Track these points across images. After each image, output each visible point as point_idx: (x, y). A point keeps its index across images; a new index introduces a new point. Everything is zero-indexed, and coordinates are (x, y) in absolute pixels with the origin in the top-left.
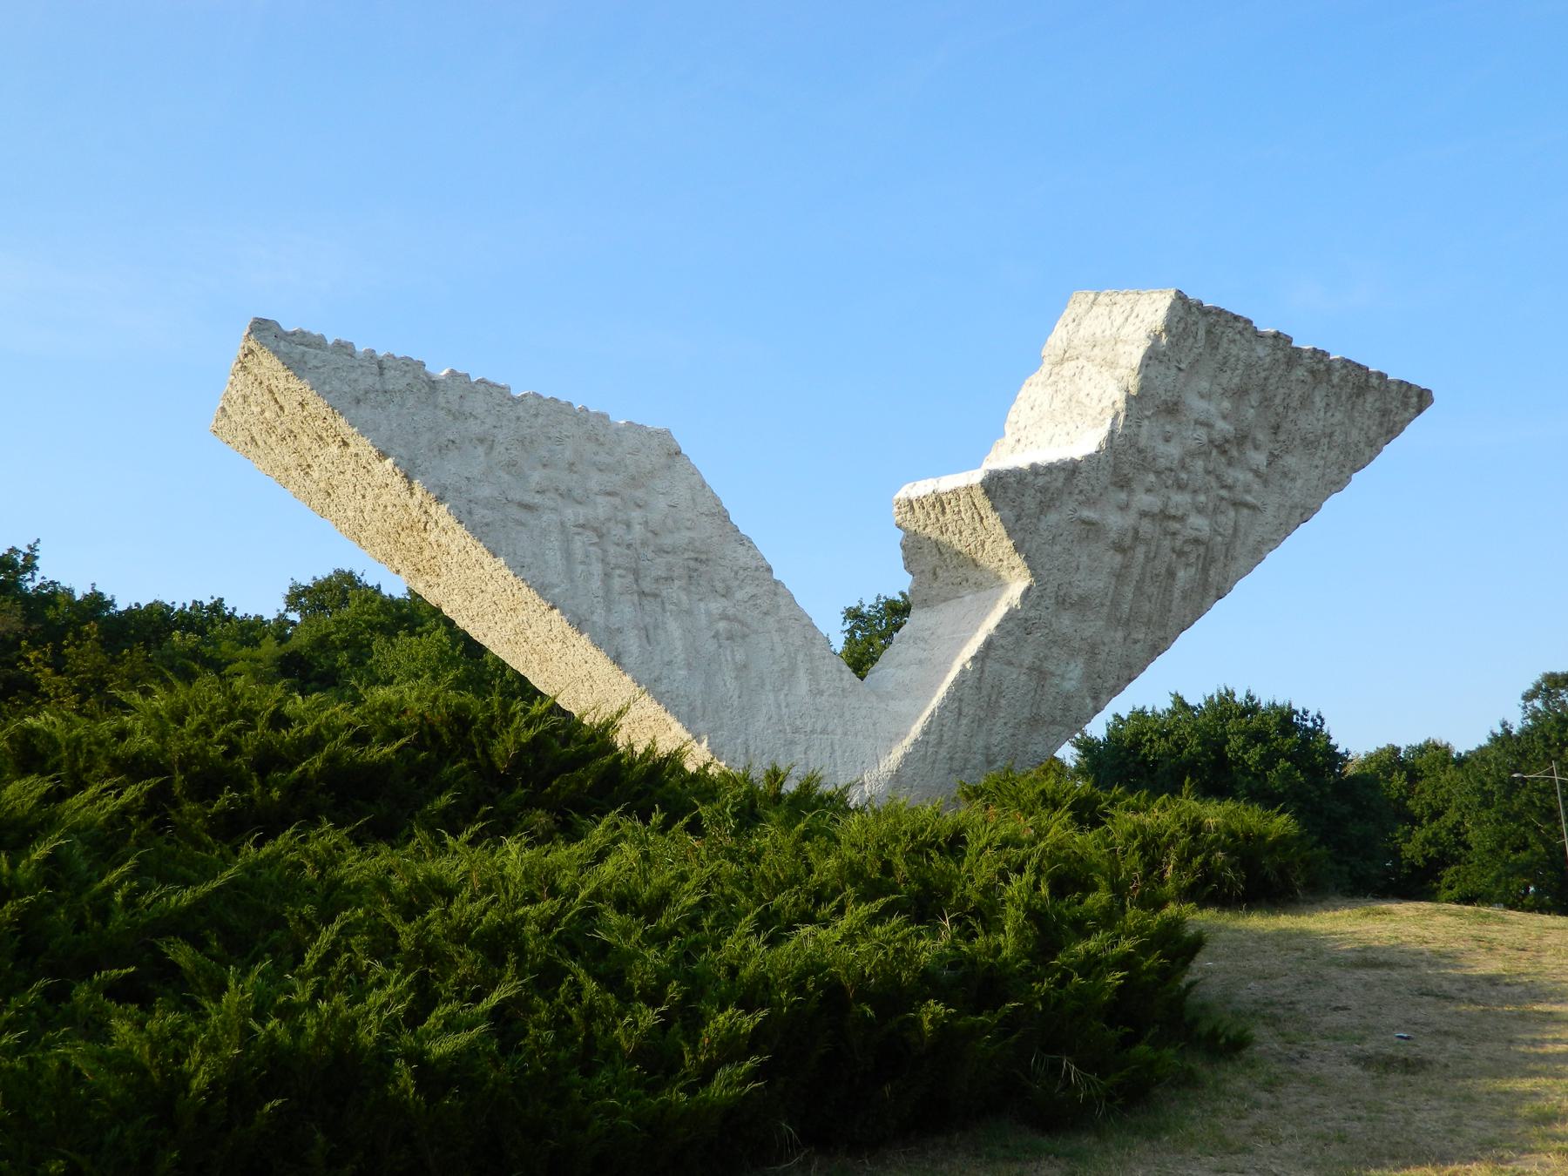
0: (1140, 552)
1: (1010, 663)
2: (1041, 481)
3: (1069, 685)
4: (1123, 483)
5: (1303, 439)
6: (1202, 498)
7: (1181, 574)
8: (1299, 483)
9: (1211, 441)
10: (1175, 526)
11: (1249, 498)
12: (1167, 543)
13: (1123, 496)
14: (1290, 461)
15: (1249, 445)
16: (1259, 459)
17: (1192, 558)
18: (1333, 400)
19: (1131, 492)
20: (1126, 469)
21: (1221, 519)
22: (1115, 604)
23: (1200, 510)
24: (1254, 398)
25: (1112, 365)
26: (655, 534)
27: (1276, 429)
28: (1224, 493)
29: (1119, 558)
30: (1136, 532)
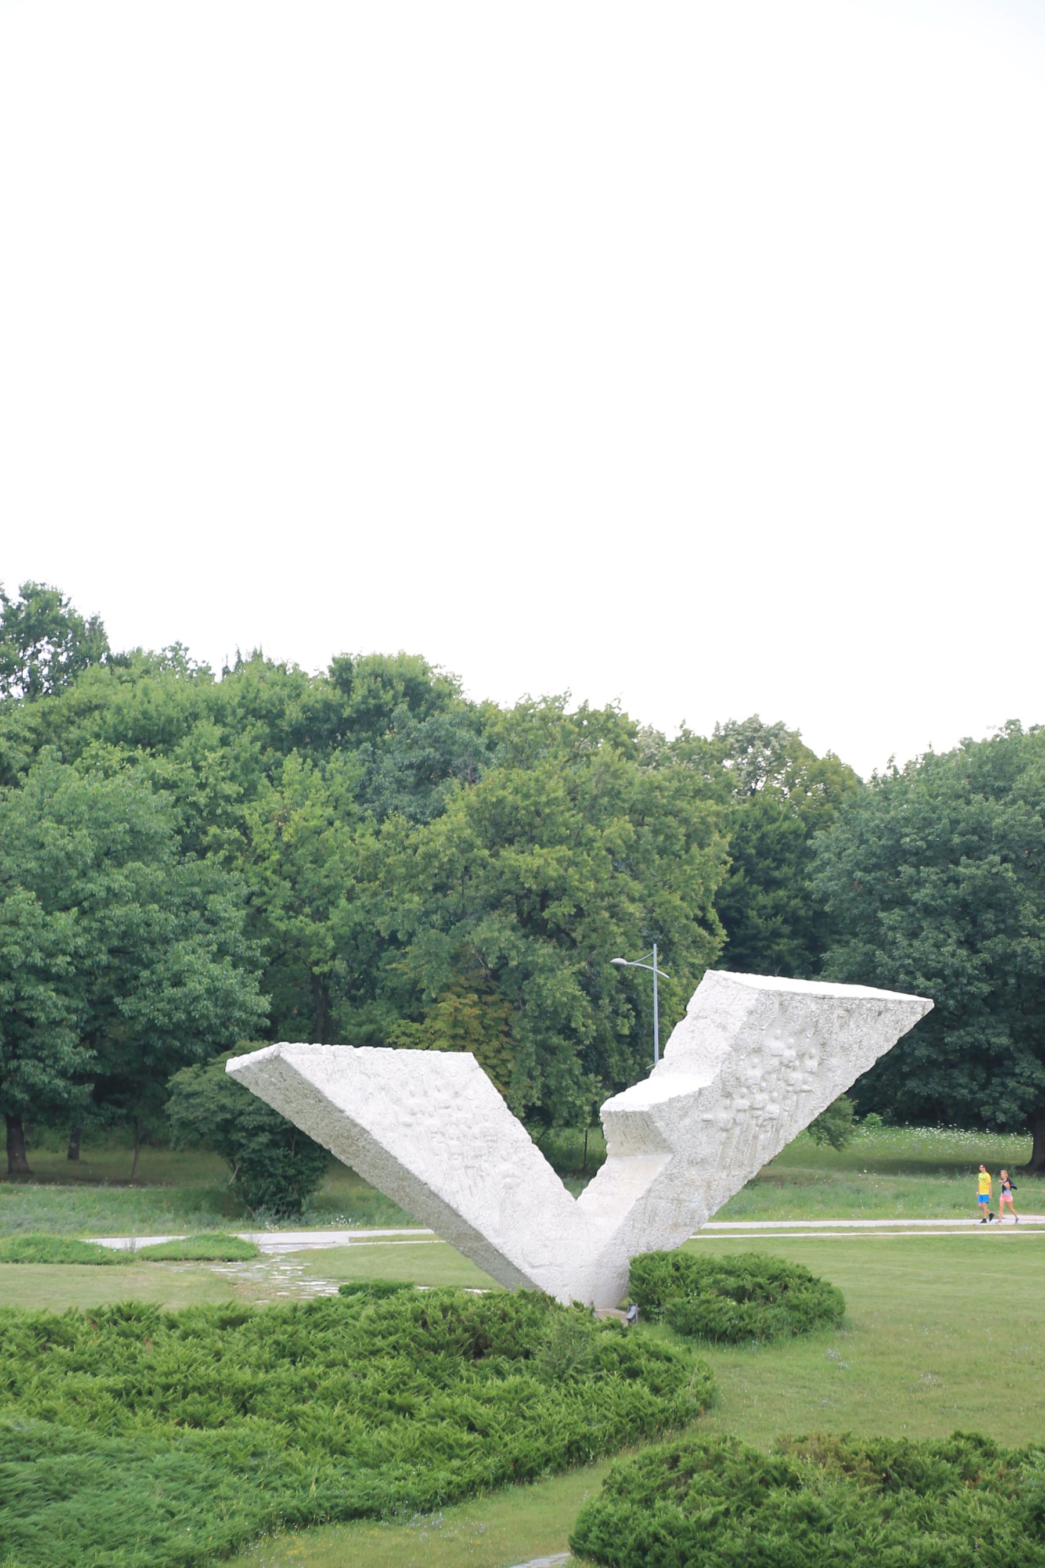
0: (737, 1131)
1: (661, 1198)
2: (679, 1105)
3: (693, 1206)
4: (728, 1095)
5: (842, 1047)
6: (775, 1094)
7: (762, 1137)
8: (839, 1072)
9: (781, 1063)
10: (759, 1112)
11: (806, 1087)
12: (754, 1122)
13: (728, 1102)
14: (834, 1061)
15: (807, 1057)
16: (812, 1064)
17: (769, 1128)
18: (862, 1022)
19: (733, 1099)
20: (730, 1089)
21: (788, 1102)
22: (722, 1158)
23: (773, 1101)
24: (809, 1033)
25: (724, 1028)
26: (470, 1128)
27: (823, 1045)
28: (790, 1088)
29: (724, 1135)
30: (735, 1120)
